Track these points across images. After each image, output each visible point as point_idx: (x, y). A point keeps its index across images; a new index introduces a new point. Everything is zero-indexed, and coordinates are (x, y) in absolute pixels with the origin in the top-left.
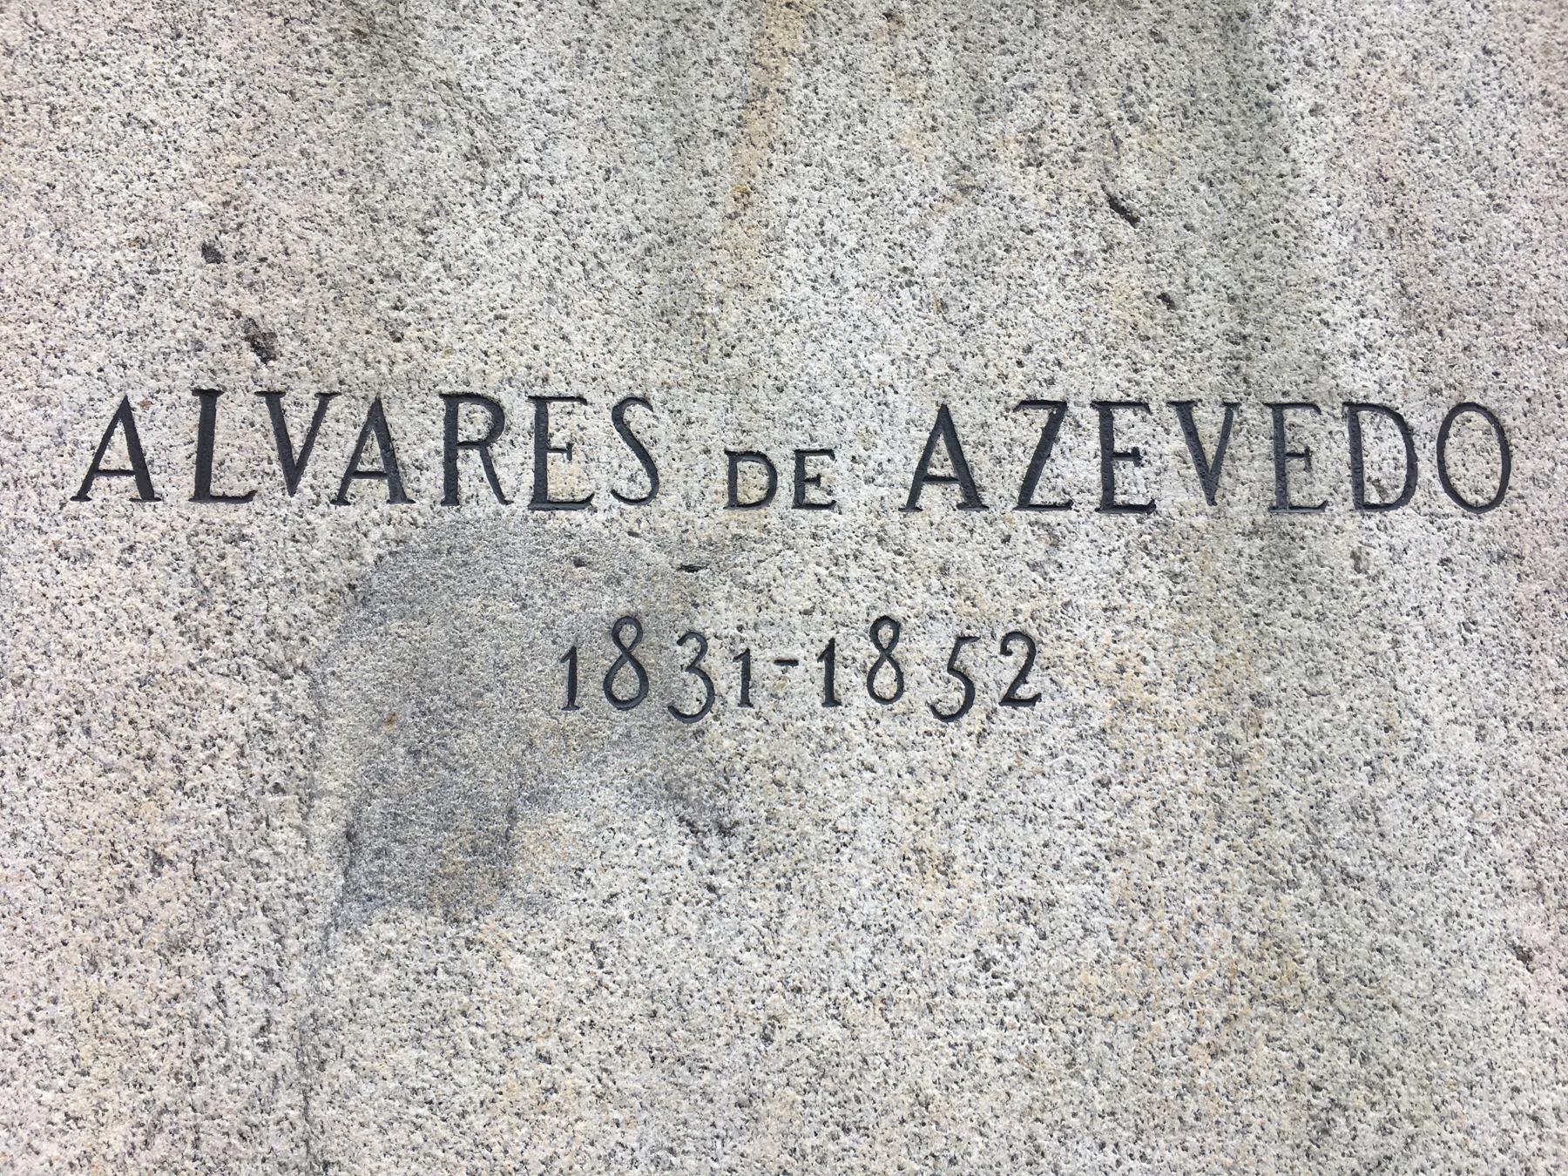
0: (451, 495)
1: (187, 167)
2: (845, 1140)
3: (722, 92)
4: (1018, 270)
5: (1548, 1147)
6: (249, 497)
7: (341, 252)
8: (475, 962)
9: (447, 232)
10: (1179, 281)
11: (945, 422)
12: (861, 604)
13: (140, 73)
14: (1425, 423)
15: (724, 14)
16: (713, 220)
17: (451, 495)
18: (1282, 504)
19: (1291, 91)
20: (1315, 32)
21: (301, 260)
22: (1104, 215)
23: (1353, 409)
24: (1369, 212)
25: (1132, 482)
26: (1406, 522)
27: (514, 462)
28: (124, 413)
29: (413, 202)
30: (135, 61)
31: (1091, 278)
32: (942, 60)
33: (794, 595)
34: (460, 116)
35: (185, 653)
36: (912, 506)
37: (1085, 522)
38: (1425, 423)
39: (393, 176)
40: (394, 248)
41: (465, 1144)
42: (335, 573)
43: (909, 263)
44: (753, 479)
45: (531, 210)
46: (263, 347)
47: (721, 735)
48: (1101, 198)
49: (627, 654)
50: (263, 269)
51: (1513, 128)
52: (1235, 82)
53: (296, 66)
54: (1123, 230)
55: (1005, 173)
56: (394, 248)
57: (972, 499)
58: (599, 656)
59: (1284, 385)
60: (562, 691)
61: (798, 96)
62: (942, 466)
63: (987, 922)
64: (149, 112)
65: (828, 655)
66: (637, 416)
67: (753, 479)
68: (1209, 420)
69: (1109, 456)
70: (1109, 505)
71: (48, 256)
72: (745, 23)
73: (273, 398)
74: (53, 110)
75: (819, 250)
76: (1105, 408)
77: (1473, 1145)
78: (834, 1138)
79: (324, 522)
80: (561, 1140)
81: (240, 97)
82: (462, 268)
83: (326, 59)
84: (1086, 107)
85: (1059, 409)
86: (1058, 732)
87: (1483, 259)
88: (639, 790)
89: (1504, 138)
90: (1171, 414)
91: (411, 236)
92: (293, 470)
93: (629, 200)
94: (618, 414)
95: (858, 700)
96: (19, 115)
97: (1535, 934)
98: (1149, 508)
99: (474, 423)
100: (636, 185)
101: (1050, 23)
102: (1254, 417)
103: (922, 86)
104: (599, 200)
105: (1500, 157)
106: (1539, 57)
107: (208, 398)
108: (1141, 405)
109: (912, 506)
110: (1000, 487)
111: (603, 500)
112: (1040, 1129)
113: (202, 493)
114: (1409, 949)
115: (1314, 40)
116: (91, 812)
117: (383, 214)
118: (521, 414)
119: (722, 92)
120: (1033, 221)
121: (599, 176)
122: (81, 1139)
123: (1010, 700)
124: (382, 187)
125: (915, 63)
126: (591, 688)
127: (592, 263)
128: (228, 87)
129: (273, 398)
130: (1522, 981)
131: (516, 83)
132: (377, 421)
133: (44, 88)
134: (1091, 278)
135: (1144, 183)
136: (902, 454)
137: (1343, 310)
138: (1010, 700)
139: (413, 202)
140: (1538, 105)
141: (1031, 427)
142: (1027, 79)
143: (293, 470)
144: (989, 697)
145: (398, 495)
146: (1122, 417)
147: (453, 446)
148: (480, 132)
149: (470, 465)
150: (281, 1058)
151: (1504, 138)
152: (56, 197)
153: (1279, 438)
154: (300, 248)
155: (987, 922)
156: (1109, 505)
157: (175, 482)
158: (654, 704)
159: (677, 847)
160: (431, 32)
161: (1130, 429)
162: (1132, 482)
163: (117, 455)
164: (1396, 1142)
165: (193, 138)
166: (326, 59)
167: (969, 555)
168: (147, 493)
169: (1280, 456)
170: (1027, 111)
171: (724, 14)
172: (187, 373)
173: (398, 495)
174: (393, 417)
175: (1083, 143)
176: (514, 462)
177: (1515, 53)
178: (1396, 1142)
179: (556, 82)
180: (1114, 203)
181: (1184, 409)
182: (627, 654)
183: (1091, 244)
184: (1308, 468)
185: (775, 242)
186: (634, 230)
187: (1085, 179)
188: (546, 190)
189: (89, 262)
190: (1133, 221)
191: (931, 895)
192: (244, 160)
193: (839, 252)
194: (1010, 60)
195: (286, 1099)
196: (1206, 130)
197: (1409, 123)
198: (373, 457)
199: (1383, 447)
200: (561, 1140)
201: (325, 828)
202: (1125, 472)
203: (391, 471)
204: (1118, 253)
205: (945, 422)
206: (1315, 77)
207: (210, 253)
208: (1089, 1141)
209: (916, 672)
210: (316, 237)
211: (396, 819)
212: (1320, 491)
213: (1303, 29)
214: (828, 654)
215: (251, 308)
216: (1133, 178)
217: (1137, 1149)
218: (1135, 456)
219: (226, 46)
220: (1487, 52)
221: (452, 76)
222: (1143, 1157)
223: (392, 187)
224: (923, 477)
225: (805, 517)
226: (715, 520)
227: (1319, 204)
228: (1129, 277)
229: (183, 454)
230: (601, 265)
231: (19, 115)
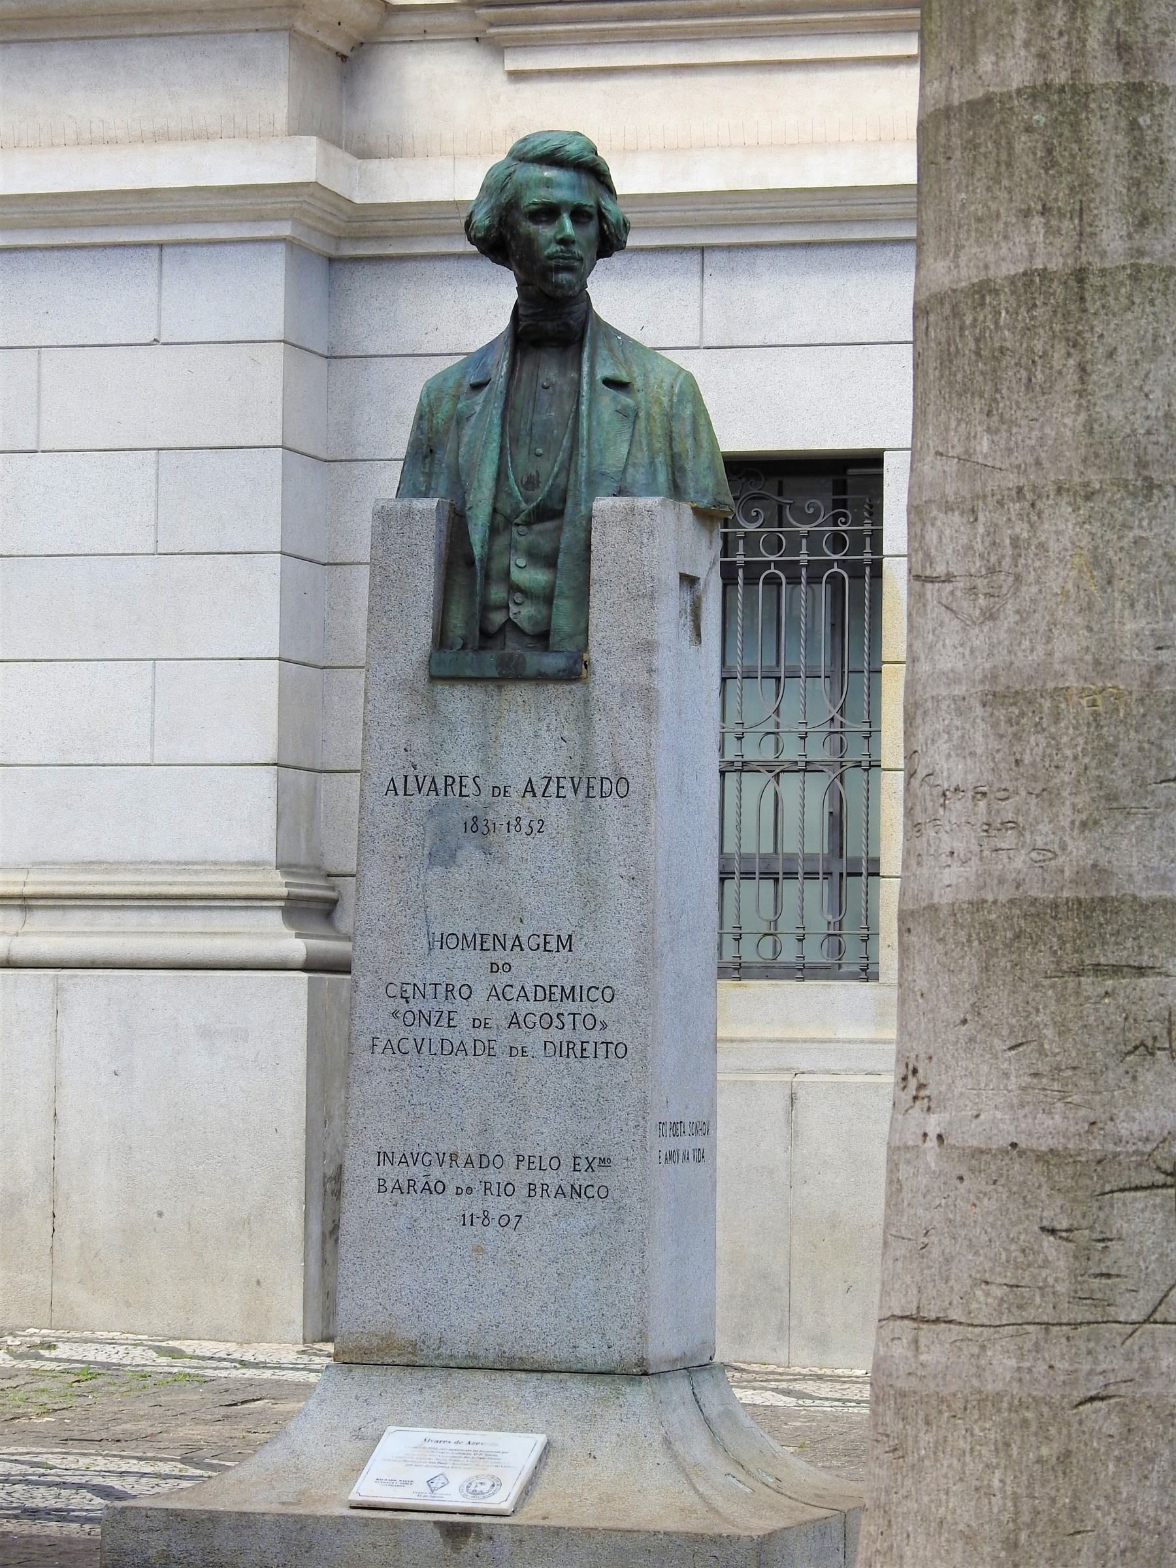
9: (445, 745)
12: (514, 814)
18: (588, 796)
25: (562, 792)
27: (456, 787)
33: (503, 813)
37: (554, 799)
42: (428, 808)
44: (497, 791)
57: (534, 795)
59: (588, 774)
63: (533, 870)
67: (497, 791)
68: (576, 780)
69: (559, 787)
86: (546, 838)
88: (476, 847)
92: (420, 790)
97: (624, 874)
99: (450, 781)
110: (539, 793)
113: (405, 794)
114: (603, 875)
116: (389, 849)
118: (458, 780)
126: (469, 829)
136: (522, 787)
137: (601, 759)
139: (439, 739)
141: (546, 781)
143: (420, 790)
155: (533, 870)
157: (401, 792)
161: (563, 782)
162: (562, 792)
163: (391, 787)
167: (533, 806)
168: (396, 794)
172: (402, 772)
176: (456, 787)
187: (557, 734)
196: (580, 724)
198: (433, 788)
199: (607, 785)
201: (426, 852)
203: (436, 790)
216: (566, 733)
226: (490, 799)
228: (564, 753)
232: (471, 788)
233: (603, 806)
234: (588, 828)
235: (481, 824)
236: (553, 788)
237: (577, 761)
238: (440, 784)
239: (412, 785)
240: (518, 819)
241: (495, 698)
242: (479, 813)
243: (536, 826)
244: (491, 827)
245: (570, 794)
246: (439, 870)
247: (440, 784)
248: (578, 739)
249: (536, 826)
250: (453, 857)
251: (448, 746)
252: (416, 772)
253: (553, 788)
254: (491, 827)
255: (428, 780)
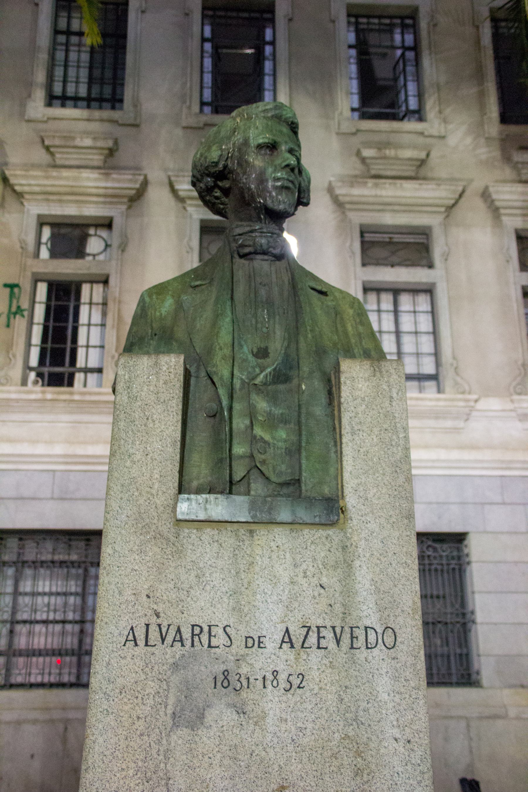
0: (193, 645)
1: (144, 579)
2: (266, 775)
3: (245, 562)
4: (302, 599)
5: (400, 779)
6: (155, 645)
7: (173, 596)
8: (197, 739)
9: (192, 592)
10: (333, 601)
11: (287, 630)
13: (134, 560)
14: (380, 631)
15: (245, 546)
16: (243, 589)
17: (193, 645)
18: (352, 648)
19: (355, 562)
20: (361, 549)
21: (165, 598)
22: (319, 587)
23: (366, 628)
24: (370, 587)
25: (323, 643)
26: (376, 651)
27: (205, 638)
28: (132, 629)
29: (186, 586)
30: (134, 557)
31: (316, 601)
32: (288, 555)
33: (258, 665)
34: (195, 568)
35: (143, 677)
36: (281, 648)
38: (380, 631)
39: (182, 580)
40: (183, 595)
41: (195, 774)
42: (171, 661)
43: (281, 598)
44: (250, 642)
45: (208, 588)
46: (158, 616)
47: (244, 694)
48: (318, 585)
49: (226, 678)
50: (158, 600)
51: (399, 569)
52: (345, 560)
53: (164, 558)
54: (322, 591)
55: (300, 580)
56: (183, 595)
57: (292, 647)
58: (221, 677)
59: (353, 623)
60: (213, 685)
61: (259, 563)
62: (286, 639)
64: (136, 568)
65: (264, 678)
66: (228, 629)
67: (250, 642)
68: (338, 630)
69: (319, 638)
70: (319, 648)
71: (118, 597)
72: (250, 548)
73: (159, 625)
74: (118, 567)
75: (263, 595)
76: (318, 627)
77: (385, 778)
78: (264, 774)
79: (169, 650)
80: (213, 774)
81: (153, 564)
82: (195, 599)
83: (170, 557)
84: (315, 566)
85: (309, 628)
86: (308, 694)
87: (392, 597)
88: (228, 705)
89: (397, 572)
90: (331, 629)
91: (185, 593)
92: (163, 640)
93: (227, 585)
94: (224, 628)
95: (270, 687)
96: (112, 568)
97: (398, 736)
98: (326, 648)
99: (197, 630)
100: (228, 582)
101: (309, 548)
102: (347, 630)
103: (284, 561)
104: (221, 585)
105: (396, 576)
106: (405, 554)
107: (147, 625)
108: (325, 627)
109: (281, 648)
110: (298, 645)
111: (221, 646)
112: (303, 773)
113: (146, 645)
114: (374, 738)
115: (360, 551)
116: (126, 708)
117: (180, 589)
118: (206, 629)
119: (245, 562)
120: (305, 589)
121: (221, 580)
122: (124, 773)
123: (299, 687)
124: (180, 582)
125: (282, 557)
126: (219, 684)
127: (220, 598)
128: (151, 562)
129: (159, 625)
130: (395, 745)
131: (205, 561)
132: (179, 630)
133: (116, 562)
134: (316, 601)
135: (326, 581)
136: (278, 637)
137: (365, 607)
138: (299, 687)
139: (186, 586)
140: (404, 565)
142: (305, 559)
143: (163, 640)
144: (295, 686)
145: (183, 645)
146: (321, 629)
147: (193, 635)
148: (199, 571)
149: (196, 639)
150: (161, 757)
151: (397, 572)
152: (119, 585)
153: (352, 634)
154: (164, 595)
156: (319, 648)
157: (141, 642)
158: (230, 688)
159: (235, 716)
160: (190, 551)
161: (324, 632)
163: (131, 637)
164: (370, 777)
165: (145, 573)
166: (170, 557)
168: (136, 645)
169: (352, 637)
170: (304, 566)
171: (245, 546)
172: (144, 621)
173: (183, 645)
174: (182, 630)
175: (315, 573)
176: (205, 638)
177: (400, 554)
178: (370, 777)
179: (213, 561)
180: (321, 586)
181: (333, 628)
182: (226, 678)
183: (316, 594)
184: (357, 640)
185: (254, 594)
186: (228, 591)
187: (315, 581)
188: (211, 583)
189: (125, 598)
190: (324, 589)
191: (283, 727)
192: (154, 577)
193: (267, 596)
194: (301, 556)
195: (162, 765)
197: (378, 569)
198: (178, 638)
199: (372, 637)
200: (213, 774)
201: (169, 711)
202: (322, 640)
203: (181, 640)
204: (321, 596)
205: (287, 630)
206: (360, 559)
207: (148, 596)
208: (312, 776)
209: (281, 681)
210: (167, 593)
211: (182, 710)
212: (359, 645)
213: (359, 549)
214: (264, 678)
215: (155, 607)
217: (321, 778)
218: (324, 637)
219: (151, 554)
220: (395, 553)
221: (193, 559)
222: (322, 779)
223: (182, 583)
224: (283, 641)
225: (259, 649)
226: (243, 651)
227: (360, 586)
228: (324, 601)
229: (143, 637)
230: (222, 598)
231: (112, 568)
232: (220, 639)
233: (370, 658)
234: (353, 682)
235: (233, 678)
236: (313, 639)
237: (338, 608)
238: (186, 634)
239: (154, 635)
240: (275, 673)
241: (247, 543)
242: (231, 666)
243: (296, 681)
244: (245, 683)
245: (332, 645)
246: (184, 732)
247: (186, 634)
248: (338, 587)
249: (296, 681)
250: (201, 717)
251: (196, 592)
252: (159, 621)
253: (313, 639)
254: (245, 683)
255: (172, 632)
